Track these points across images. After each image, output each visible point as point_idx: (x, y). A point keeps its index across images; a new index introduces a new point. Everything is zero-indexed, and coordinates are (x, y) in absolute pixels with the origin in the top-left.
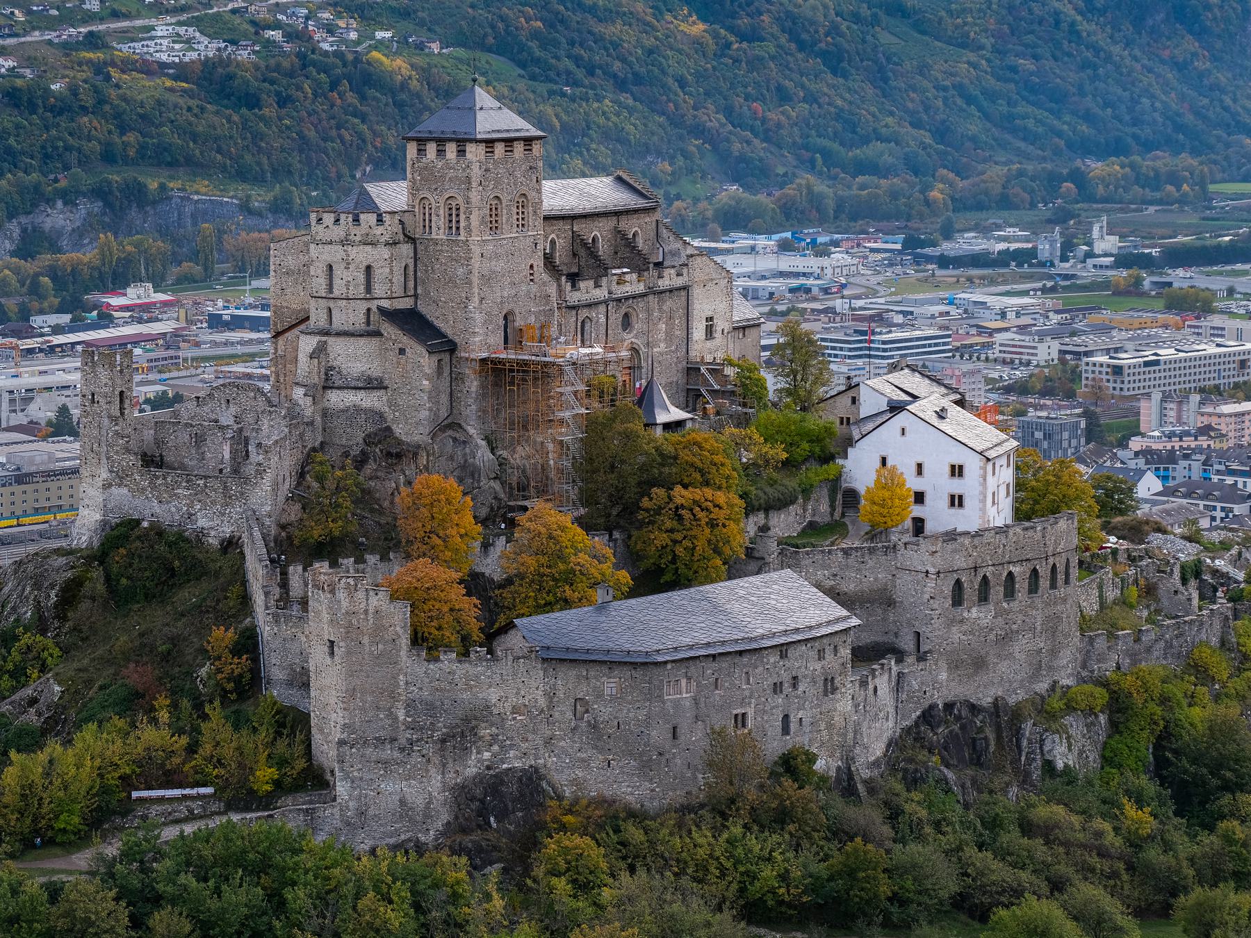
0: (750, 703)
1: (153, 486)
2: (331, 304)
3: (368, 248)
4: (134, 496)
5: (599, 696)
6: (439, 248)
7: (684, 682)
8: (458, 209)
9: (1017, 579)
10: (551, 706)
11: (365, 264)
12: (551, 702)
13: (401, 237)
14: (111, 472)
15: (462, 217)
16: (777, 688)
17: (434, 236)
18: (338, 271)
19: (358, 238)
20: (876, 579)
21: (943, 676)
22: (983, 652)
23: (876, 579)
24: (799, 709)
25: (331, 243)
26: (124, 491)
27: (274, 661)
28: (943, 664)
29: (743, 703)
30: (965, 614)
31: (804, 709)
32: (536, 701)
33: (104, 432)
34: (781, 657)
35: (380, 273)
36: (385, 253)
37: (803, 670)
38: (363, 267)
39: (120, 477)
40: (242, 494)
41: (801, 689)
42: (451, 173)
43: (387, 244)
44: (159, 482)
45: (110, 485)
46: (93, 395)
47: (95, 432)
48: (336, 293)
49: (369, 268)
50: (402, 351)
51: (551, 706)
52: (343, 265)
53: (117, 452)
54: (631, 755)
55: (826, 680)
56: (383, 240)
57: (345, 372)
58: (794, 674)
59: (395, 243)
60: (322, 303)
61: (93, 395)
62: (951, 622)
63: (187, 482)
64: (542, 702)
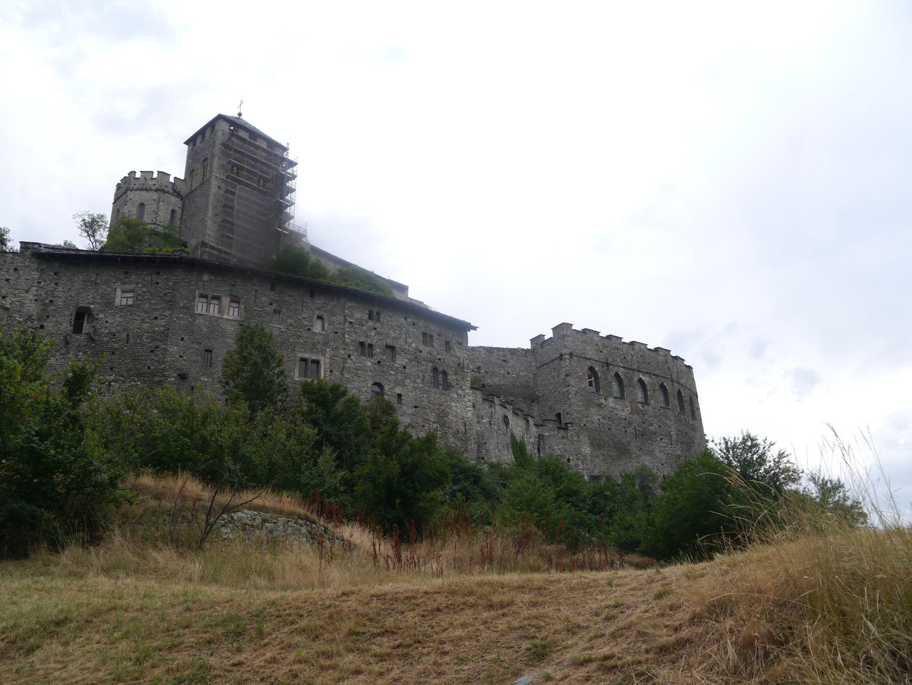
0: (323, 353)
3: (143, 193)
5: (109, 303)
7: (226, 300)
9: (648, 388)
10: (44, 316)
11: (139, 202)
12: (44, 310)
13: (171, 191)
16: (365, 348)
19: (136, 187)
20: (519, 376)
21: (587, 450)
22: (624, 441)
23: (519, 376)
24: (397, 383)
28: (584, 438)
29: (313, 348)
30: (603, 401)
31: (404, 386)
32: (22, 305)
34: (370, 318)
35: (148, 208)
36: (155, 196)
37: (401, 342)
38: (137, 204)
41: (400, 361)
43: (157, 190)
49: (142, 205)
51: (44, 316)
54: (140, 375)
55: (435, 370)
56: (154, 188)
58: (390, 342)
59: (164, 192)
62: (588, 403)
64: (32, 308)
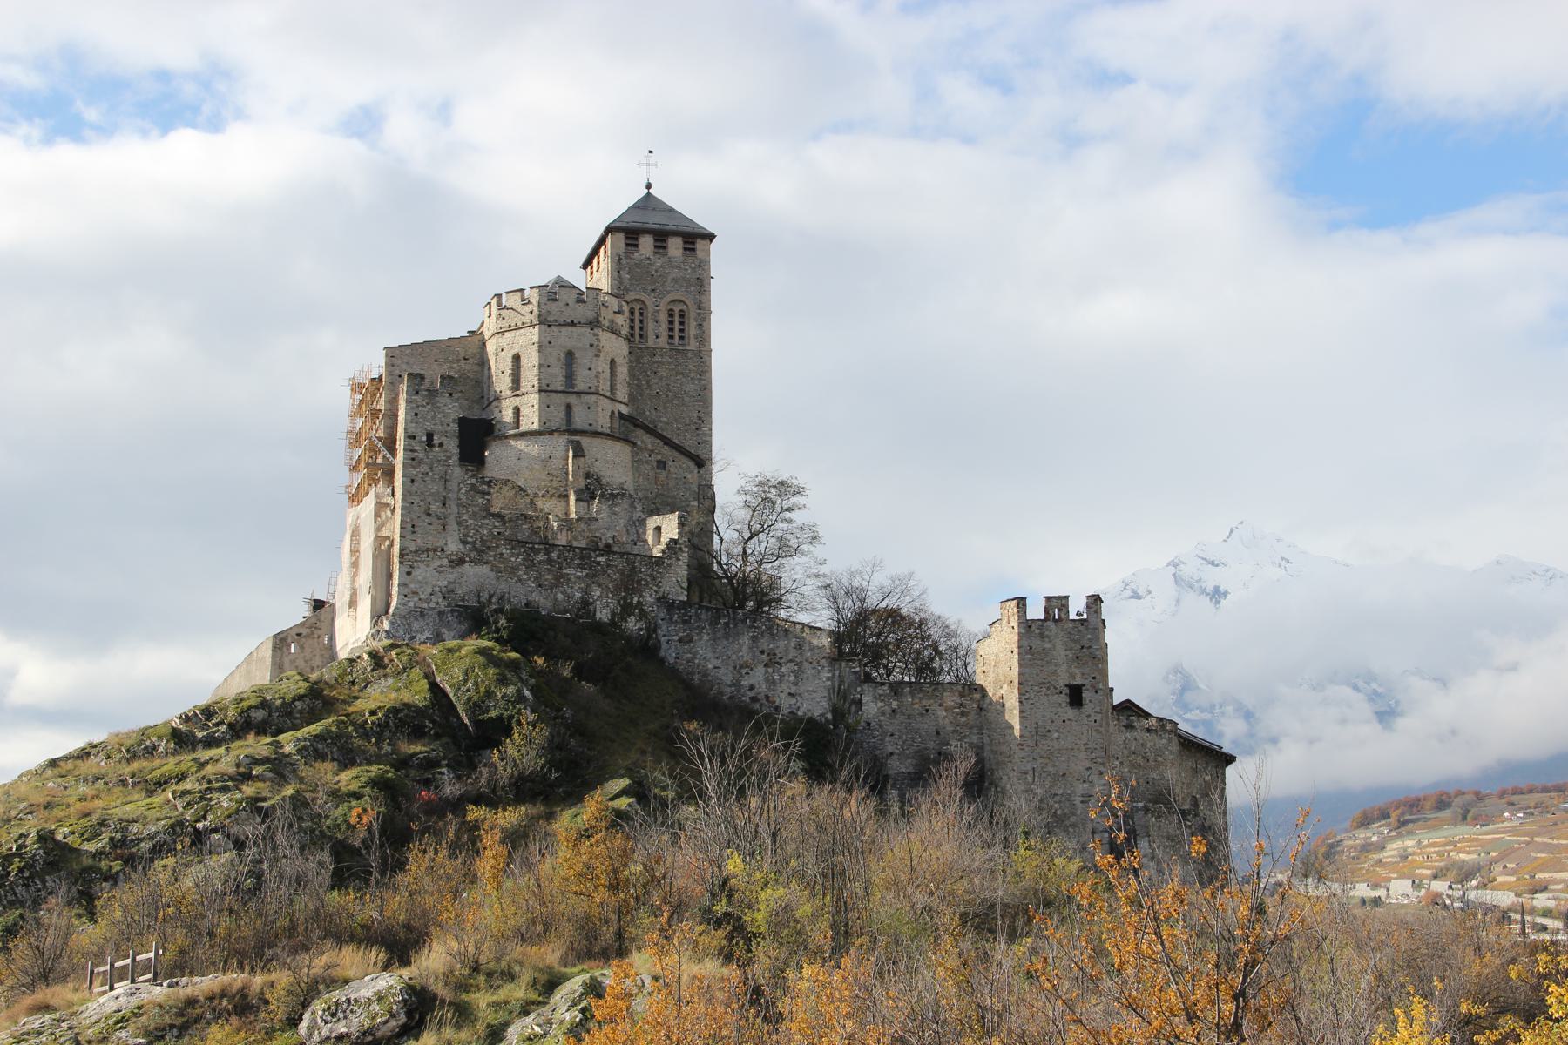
1: (530, 565)
2: (572, 399)
4: (498, 578)
6: (657, 358)
8: (682, 316)
14: (464, 542)
15: (693, 324)
17: (651, 344)
18: (583, 359)
25: (573, 324)
26: (485, 569)
27: (890, 749)
33: (453, 486)
39: (479, 551)
40: (654, 579)
42: (675, 273)
44: (540, 557)
45: (461, 562)
46: (430, 436)
47: (436, 487)
48: (580, 385)
50: (662, 464)
52: (591, 352)
53: (474, 516)
57: (604, 481)
60: (561, 399)
61: (430, 436)
63: (582, 558)
